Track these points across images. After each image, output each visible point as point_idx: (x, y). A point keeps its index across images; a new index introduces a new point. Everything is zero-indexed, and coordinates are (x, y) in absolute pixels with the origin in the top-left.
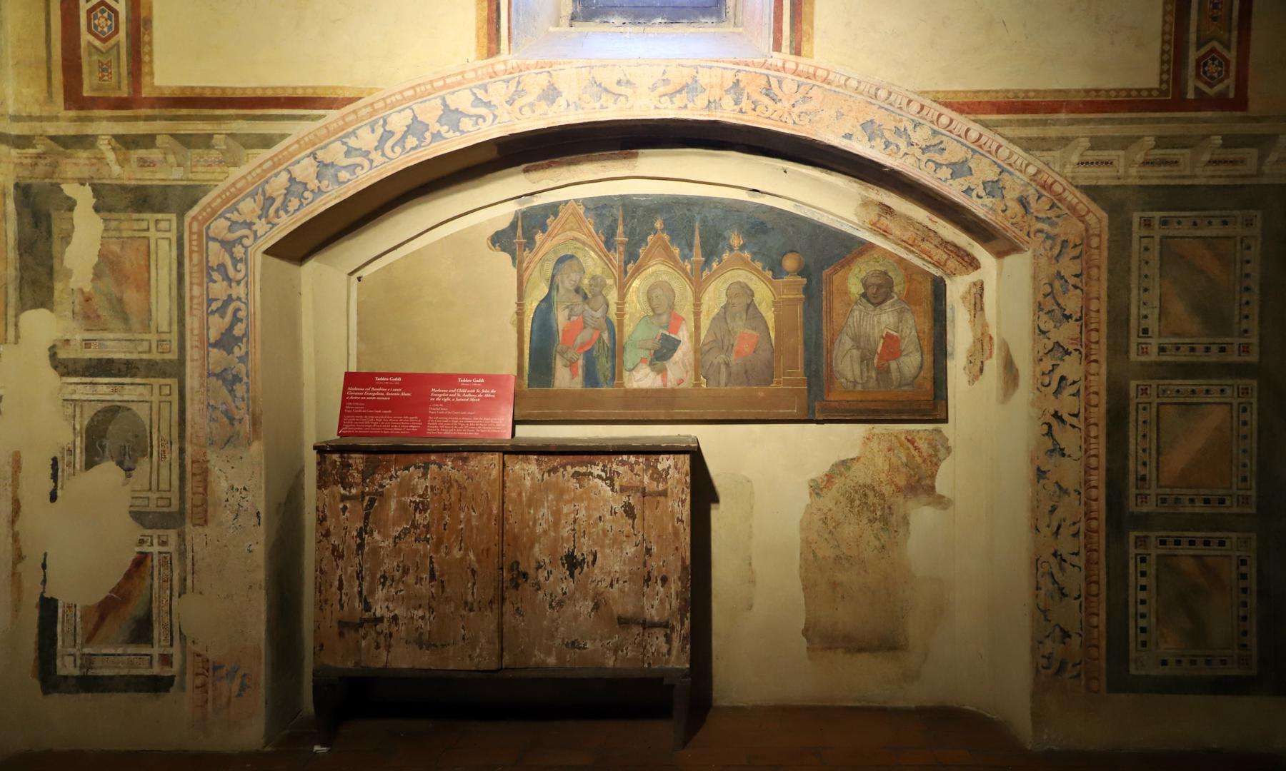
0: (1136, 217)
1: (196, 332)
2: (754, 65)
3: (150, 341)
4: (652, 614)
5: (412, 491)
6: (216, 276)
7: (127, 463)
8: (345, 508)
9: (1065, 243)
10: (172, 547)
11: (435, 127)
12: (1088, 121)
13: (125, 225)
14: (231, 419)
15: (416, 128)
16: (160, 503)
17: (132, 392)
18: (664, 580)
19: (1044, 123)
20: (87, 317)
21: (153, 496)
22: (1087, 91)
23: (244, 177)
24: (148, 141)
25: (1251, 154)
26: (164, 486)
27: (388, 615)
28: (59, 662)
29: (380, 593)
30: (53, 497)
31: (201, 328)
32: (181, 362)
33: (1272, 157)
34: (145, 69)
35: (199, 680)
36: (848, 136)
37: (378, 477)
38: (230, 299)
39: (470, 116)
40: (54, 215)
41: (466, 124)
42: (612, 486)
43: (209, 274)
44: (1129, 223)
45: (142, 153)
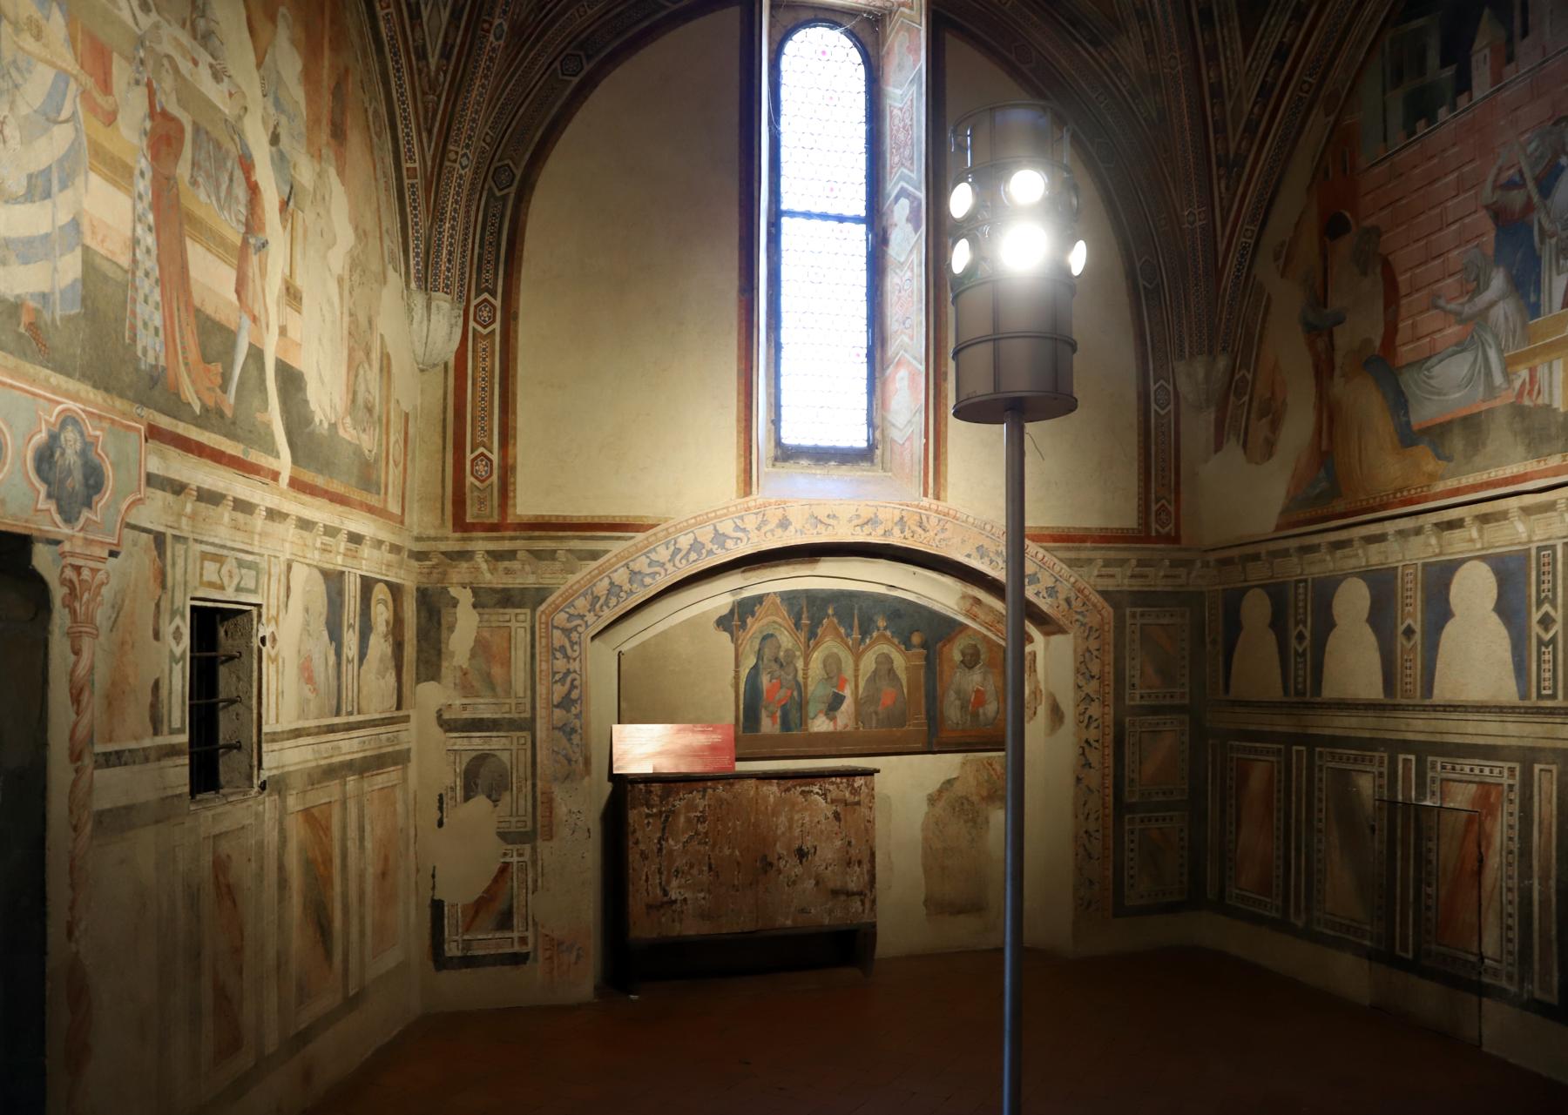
0: (1128, 611)
1: (544, 697)
2: (911, 506)
3: (510, 704)
4: (852, 886)
5: (695, 808)
6: (558, 655)
7: (494, 797)
8: (649, 823)
9: (1091, 628)
10: (526, 858)
11: (709, 546)
12: (1102, 548)
13: (494, 618)
14: (569, 761)
15: (696, 546)
16: (519, 825)
17: (496, 743)
18: (860, 863)
19: (1078, 549)
20: (464, 687)
21: (514, 820)
22: (1101, 529)
23: (578, 582)
24: (511, 554)
25: (1182, 571)
26: (521, 812)
27: (680, 898)
28: (446, 947)
29: (675, 883)
30: (440, 824)
31: (548, 694)
32: (533, 719)
33: (1194, 574)
34: (510, 502)
35: (548, 954)
36: (969, 556)
37: (671, 799)
38: (568, 672)
39: (731, 538)
40: (443, 611)
41: (730, 544)
42: (825, 799)
43: (554, 654)
44: (1124, 615)
45: (506, 564)
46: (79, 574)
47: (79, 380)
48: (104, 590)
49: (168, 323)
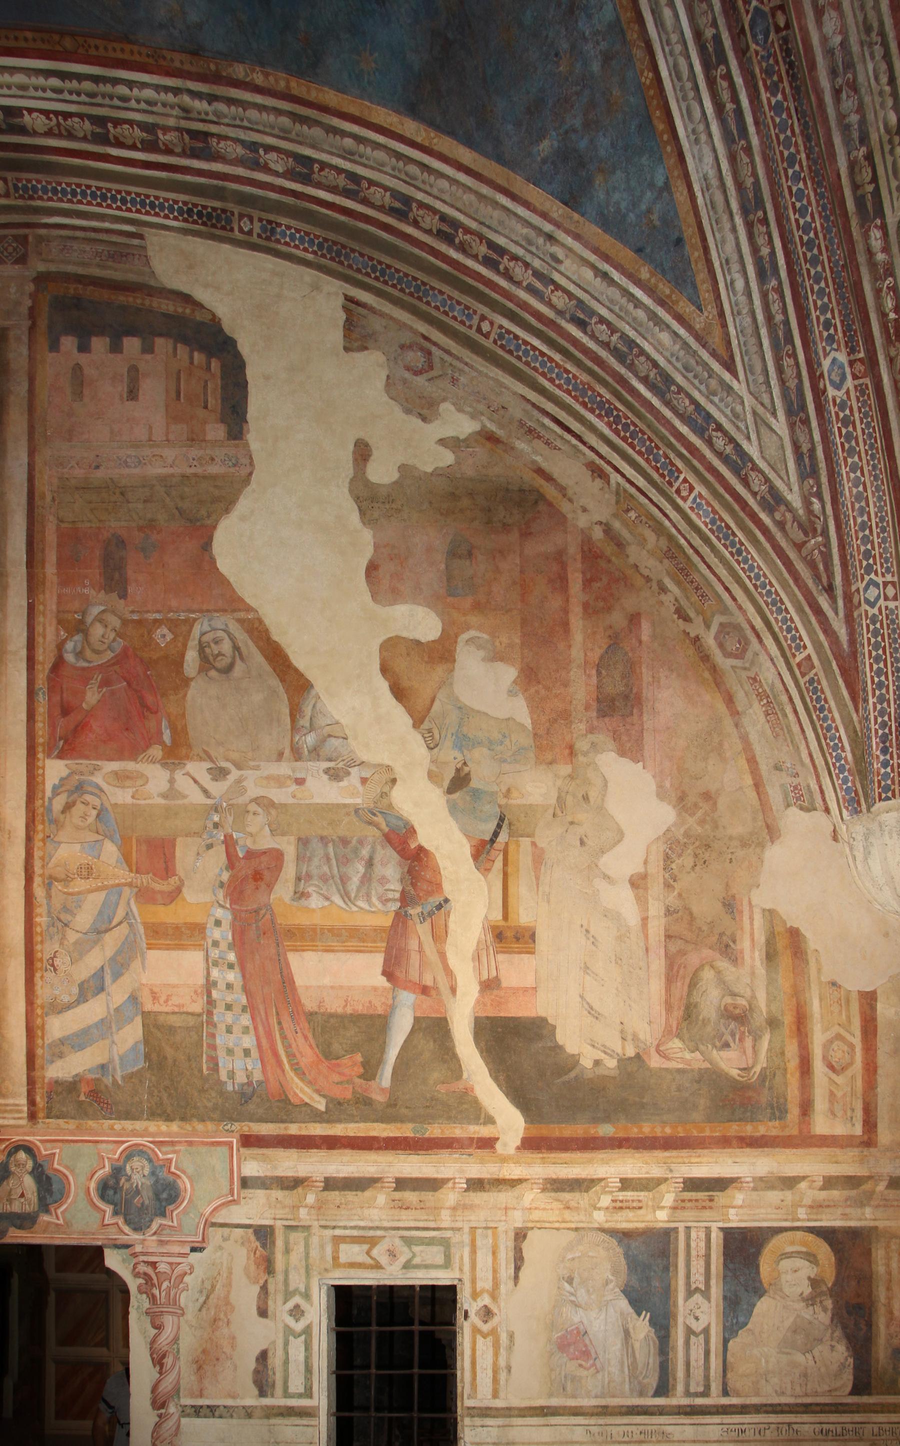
46: (155, 1268)
47: (148, 1119)
48: (187, 1279)
49: (264, 1042)
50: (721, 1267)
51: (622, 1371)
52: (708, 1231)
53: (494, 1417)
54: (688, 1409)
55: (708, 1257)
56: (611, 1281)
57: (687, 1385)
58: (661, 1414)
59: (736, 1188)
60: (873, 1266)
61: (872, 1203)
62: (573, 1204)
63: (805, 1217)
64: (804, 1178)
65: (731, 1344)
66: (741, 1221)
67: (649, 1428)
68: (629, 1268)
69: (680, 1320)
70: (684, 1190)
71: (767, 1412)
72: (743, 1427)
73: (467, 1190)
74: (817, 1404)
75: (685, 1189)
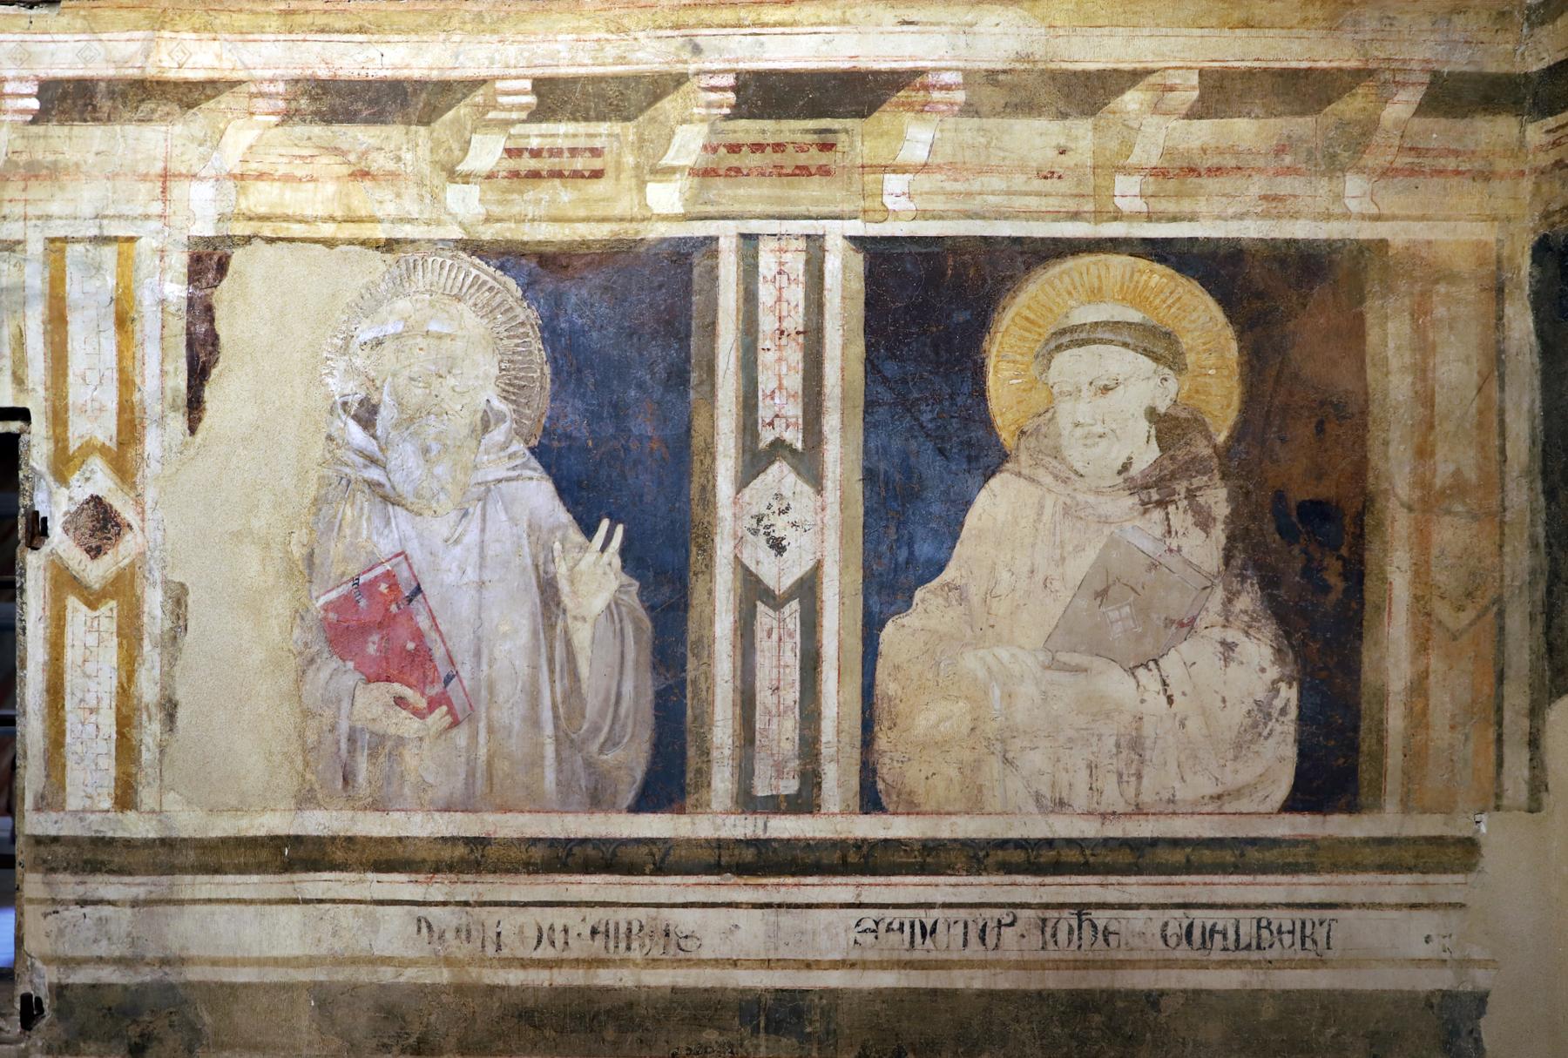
50: (858, 370)
51: (534, 722)
52: (815, 247)
53: (121, 871)
54: (749, 855)
55: (813, 336)
56: (501, 418)
57: (745, 773)
58: (660, 869)
59: (909, 106)
60: (1371, 374)
61: (1369, 160)
62: (379, 162)
63: (1139, 205)
64: (1135, 77)
65: (889, 633)
66: (922, 215)
67: (623, 915)
68: (556, 372)
69: (723, 550)
70: (738, 112)
71: (1007, 868)
72: (929, 917)
73: (38, 118)
74: (1175, 843)
75: (740, 111)
